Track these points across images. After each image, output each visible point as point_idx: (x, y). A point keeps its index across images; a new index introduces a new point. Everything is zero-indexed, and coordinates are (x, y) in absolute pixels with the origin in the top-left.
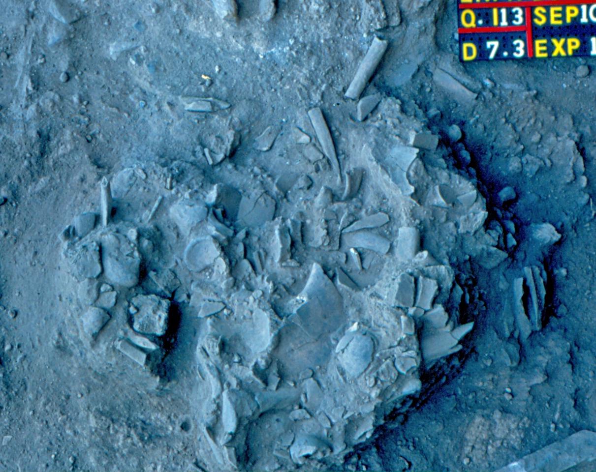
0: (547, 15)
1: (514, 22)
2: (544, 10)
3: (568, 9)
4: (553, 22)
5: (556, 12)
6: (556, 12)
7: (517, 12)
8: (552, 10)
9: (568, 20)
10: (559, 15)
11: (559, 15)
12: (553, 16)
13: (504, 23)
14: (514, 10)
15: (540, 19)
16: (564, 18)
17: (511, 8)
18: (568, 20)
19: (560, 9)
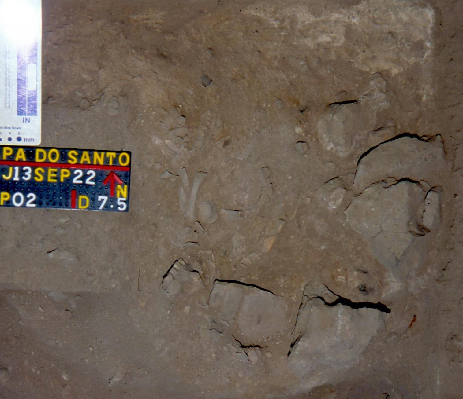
0: (45, 175)
1: (24, 178)
2: (43, 171)
3: (63, 170)
4: (50, 180)
5: (52, 173)
6: (52, 173)
7: (27, 170)
8: (50, 170)
9: (62, 180)
10: (54, 175)
11: (54, 175)
12: (50, 175)
13: (16, 178)
14: (25, 168)
15: (39, 177)
16: (58, 178)
17: (23, 166)
18: (62, 180)
19: (55, 170)
